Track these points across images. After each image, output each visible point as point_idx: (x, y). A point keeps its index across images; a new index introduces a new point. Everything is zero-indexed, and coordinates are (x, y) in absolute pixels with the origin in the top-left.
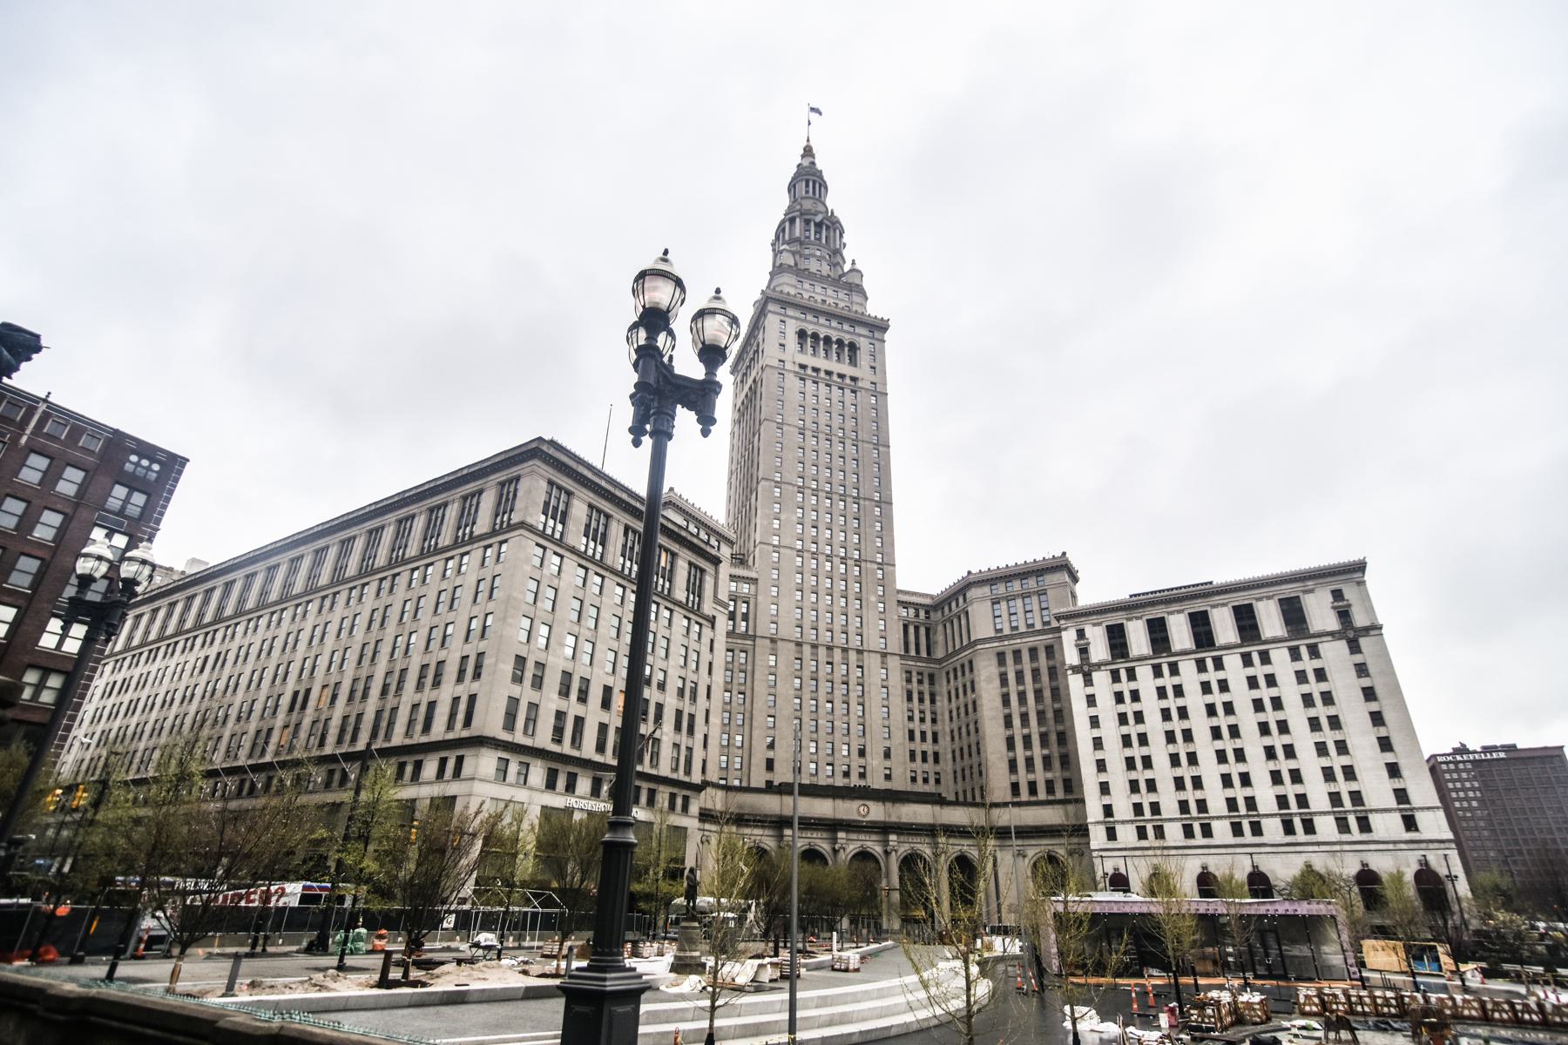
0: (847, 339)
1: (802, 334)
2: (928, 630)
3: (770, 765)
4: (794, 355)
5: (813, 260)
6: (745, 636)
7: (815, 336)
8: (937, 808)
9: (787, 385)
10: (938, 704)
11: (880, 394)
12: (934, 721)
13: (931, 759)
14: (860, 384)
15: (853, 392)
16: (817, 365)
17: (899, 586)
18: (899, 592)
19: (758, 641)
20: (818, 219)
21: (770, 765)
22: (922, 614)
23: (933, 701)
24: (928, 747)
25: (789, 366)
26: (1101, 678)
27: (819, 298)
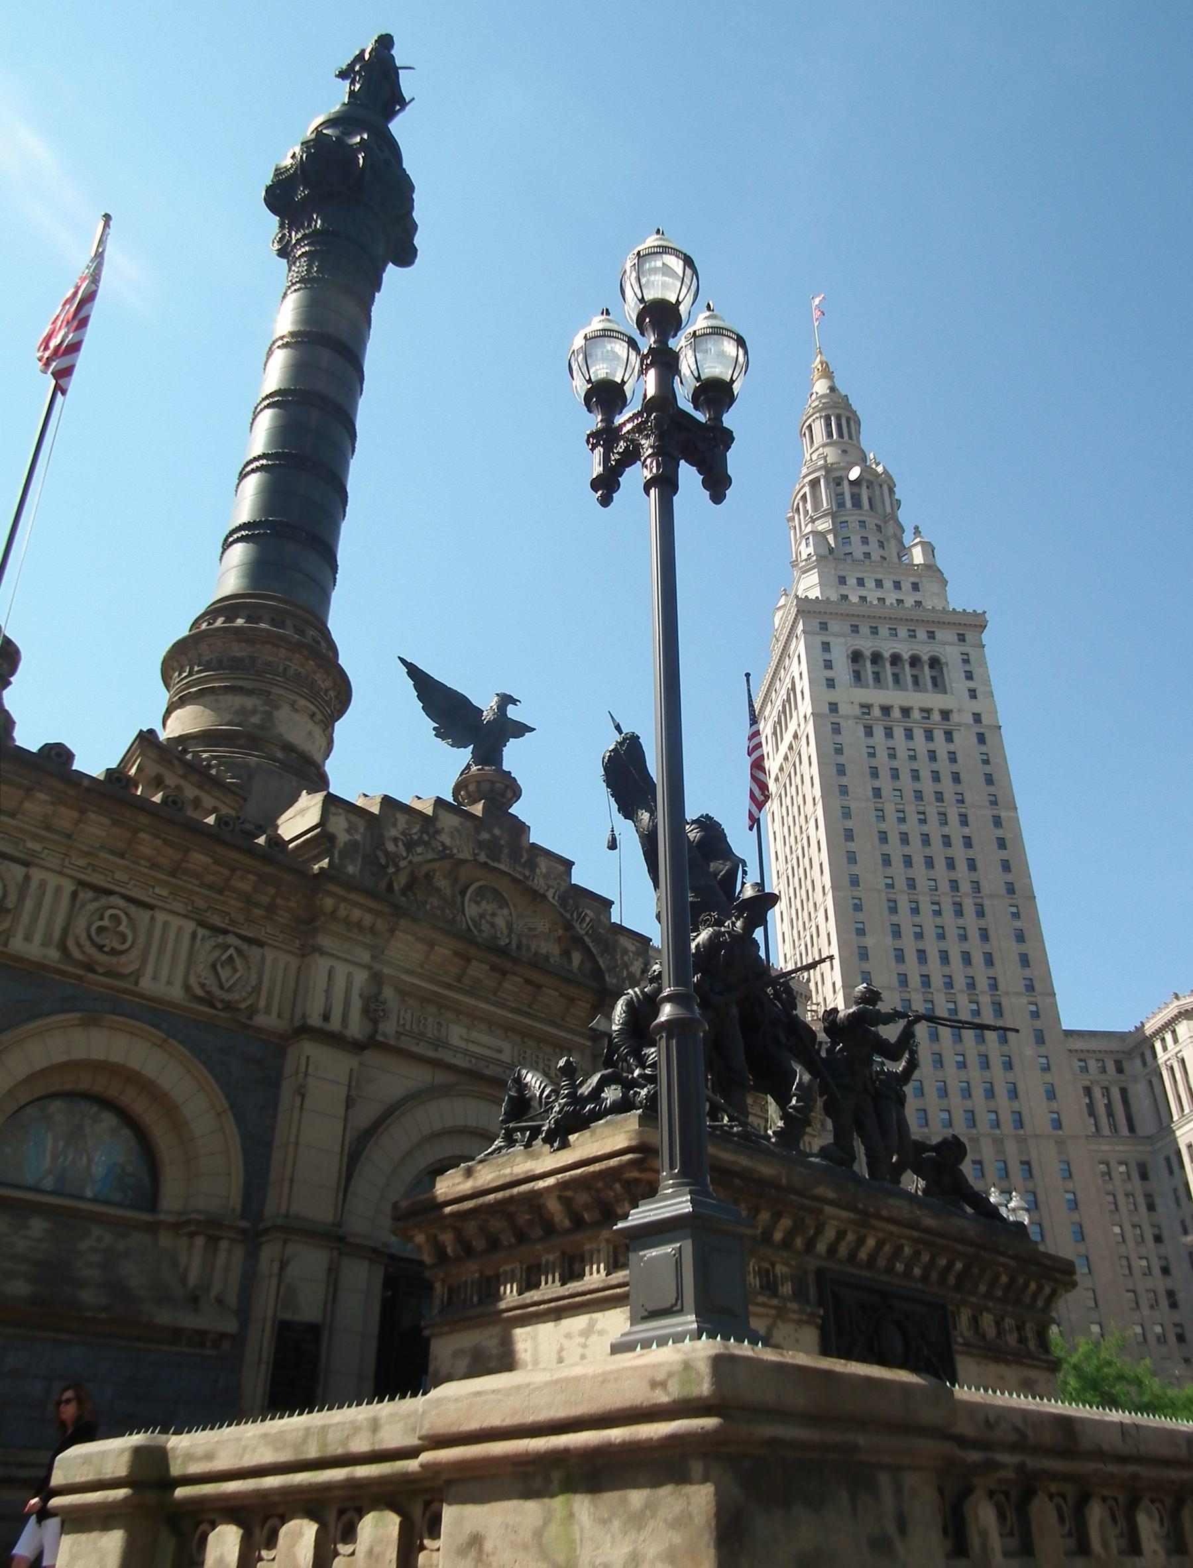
0: (925, 653)
1: (856, 657)
2: (1124, 1092)
4: (850, 697)
5: (856, 539)
7: (876, 658)
10: (1160, 1209)
13: (1164, 1303)
14: (955, 718)
16: (887, 702)
17: (1065, 1026)
18: (1069, 1033)
20: (854, 473)
22: (1111, 1067)
23: (1151, 1207)
25: (842, 709)
27: (873, 596)
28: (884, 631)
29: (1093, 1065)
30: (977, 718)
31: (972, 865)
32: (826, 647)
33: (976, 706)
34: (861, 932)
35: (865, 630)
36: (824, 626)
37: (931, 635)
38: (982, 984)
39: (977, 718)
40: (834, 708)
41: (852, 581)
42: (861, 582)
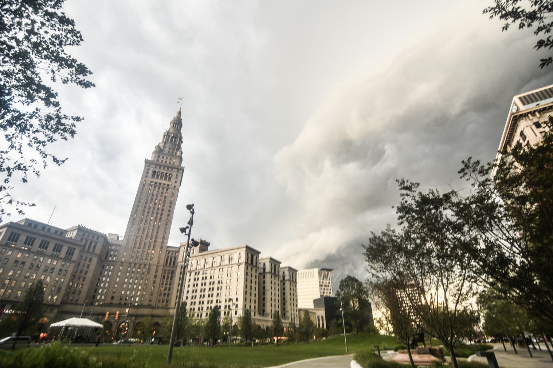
0: (169, 173)
1: (155, 172)
2: (175, 258)
3: (113, 298)
4: (149, 179)
6: (113, 261)
8: (151, 310)
9: (145, 187)
11: (176, 189)
12: (170, 284)
13: (166, 295)
15: (167, 189)
17: (169, 245)
18: (168, 247)
19: (117, 263)
20: (172, 135)
21: (113, 298)
22: (174, 254)
24: (167, 292)
26: (193, 274)
28: (162, 168)
29: (171, 253)
30: (175, 187)
31: (162, 214)
32: (148, 169)
33: (174, 184)
34: (133, 224)
35: (158, 167)
36: (149, 166)
37: (172, 169)
38: (154, 236)
39: (175, 187)
40: (145, 181)
41: (161, 157)
42: (163, 157)
